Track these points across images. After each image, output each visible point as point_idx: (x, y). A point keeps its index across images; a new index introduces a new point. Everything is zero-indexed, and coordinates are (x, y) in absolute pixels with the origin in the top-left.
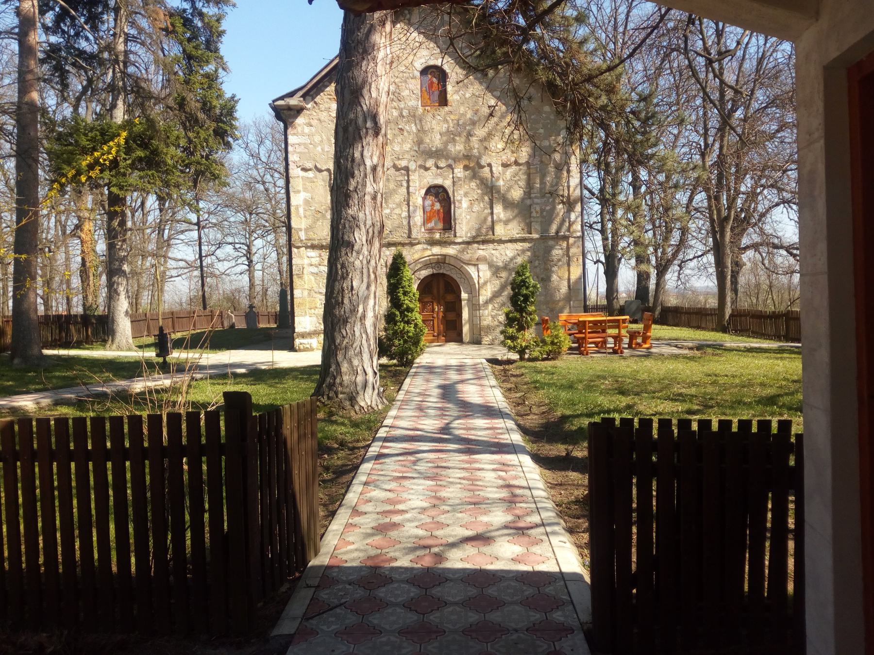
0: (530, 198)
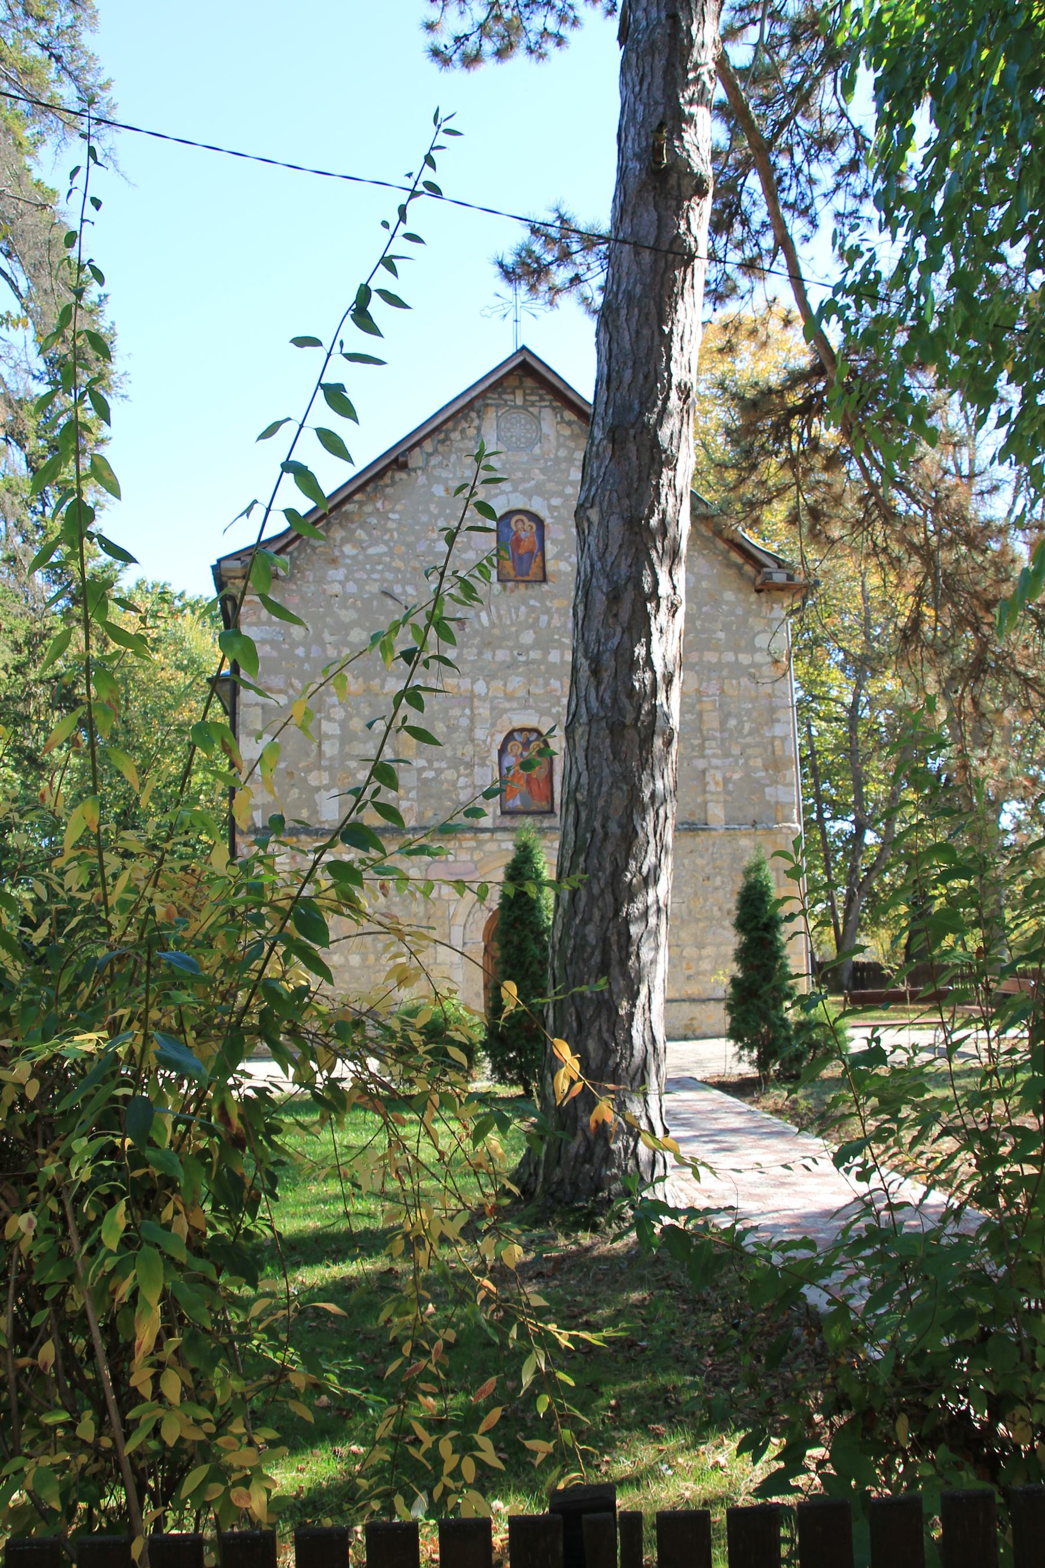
0: (703, 757)
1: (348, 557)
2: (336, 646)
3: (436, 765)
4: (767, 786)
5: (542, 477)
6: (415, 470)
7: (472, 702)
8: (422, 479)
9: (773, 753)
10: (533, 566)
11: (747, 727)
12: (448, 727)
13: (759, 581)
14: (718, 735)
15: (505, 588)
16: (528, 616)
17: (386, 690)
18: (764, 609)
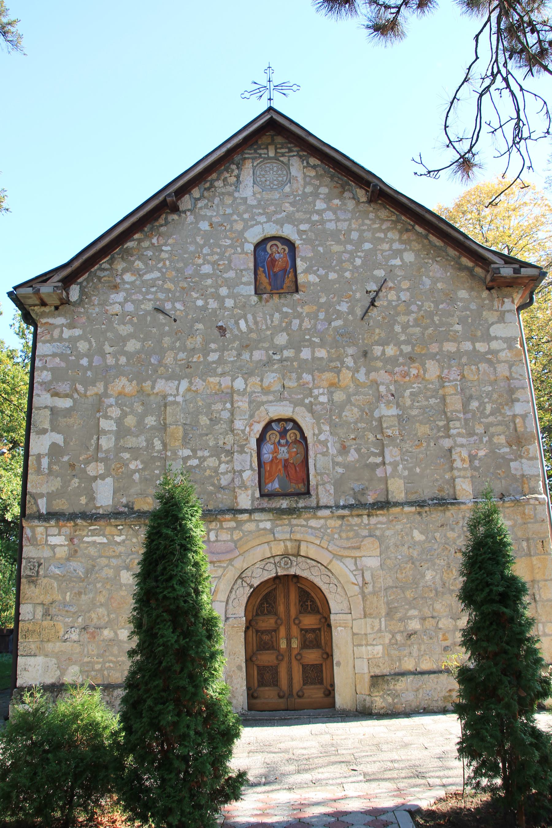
0: (449, 436)
1: (127, 283)
2: (115, 355)
3: (200, 454)
4: (512, 460)
5: (292, 209)
6: (185, 212)
7: (232, 397)
8: (190, 218)
9: (516, 431)
10: (286, 281)
11: (489, 408)
12: (211, 420)
13: (489, 278)
14: (461, 415)
15: (260, 299)
16: (281, 322)
17: (155, 391)
18: (496, 303)
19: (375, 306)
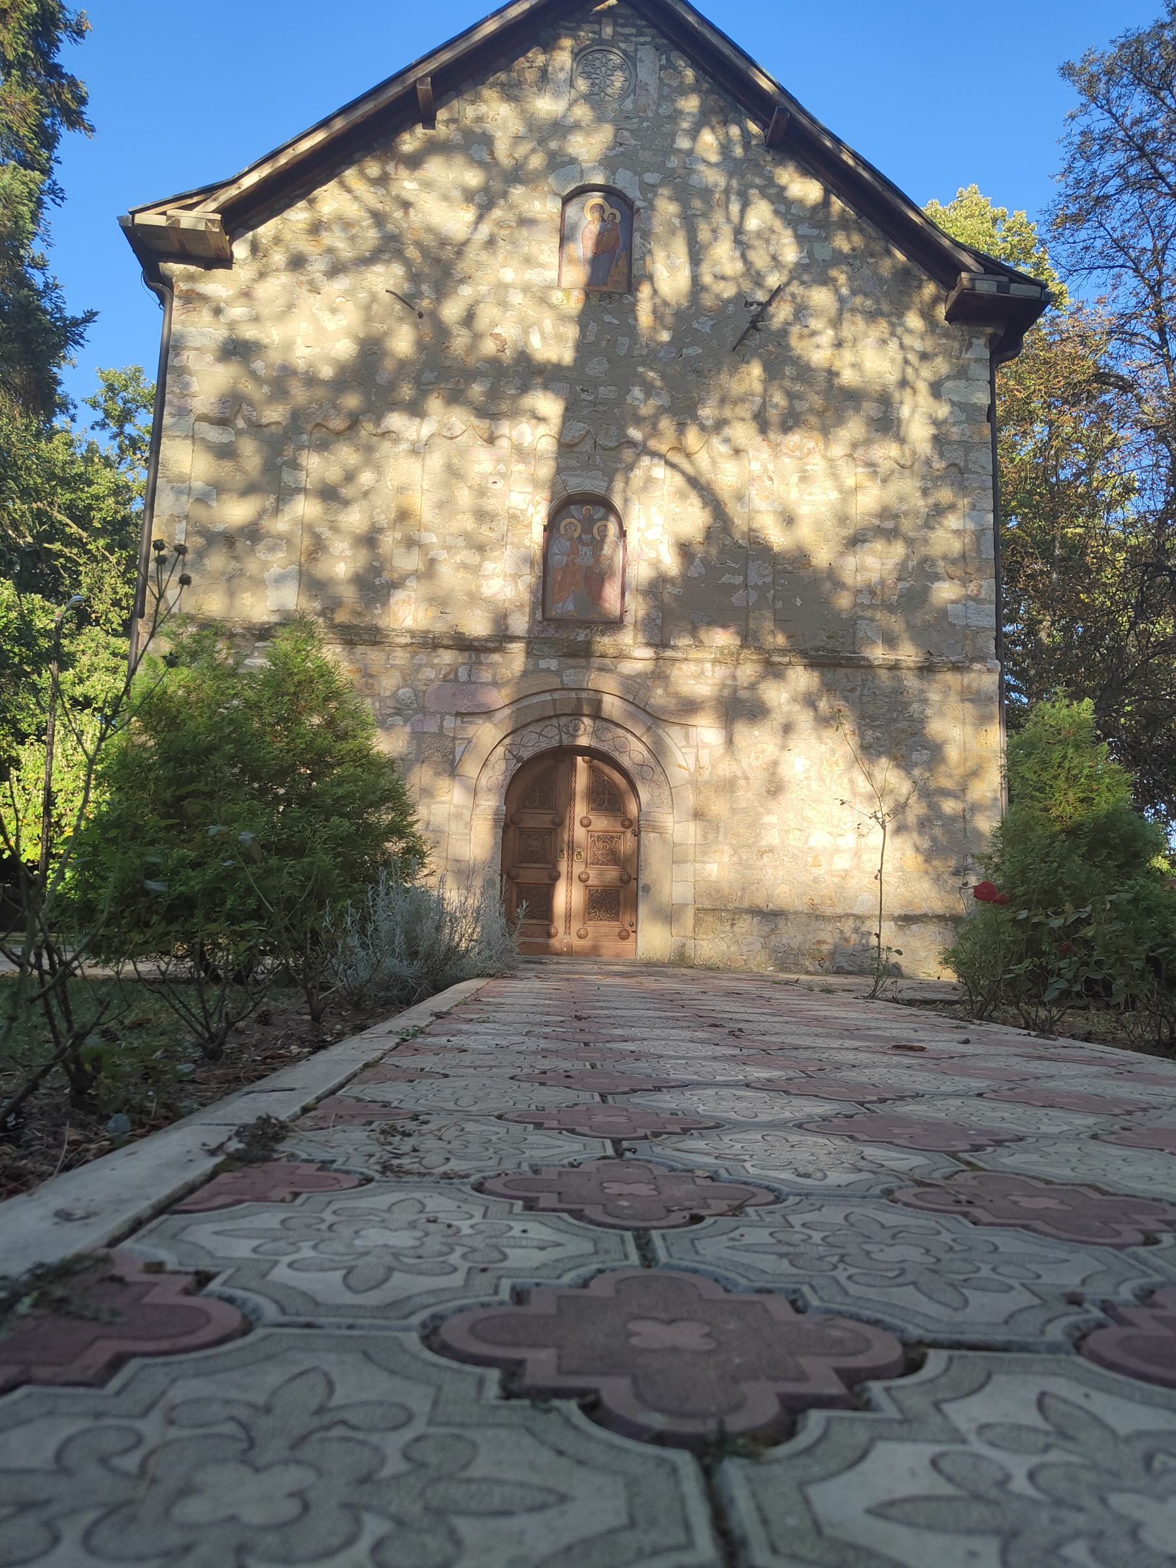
5: (633, 142)
19: (758, 330)
